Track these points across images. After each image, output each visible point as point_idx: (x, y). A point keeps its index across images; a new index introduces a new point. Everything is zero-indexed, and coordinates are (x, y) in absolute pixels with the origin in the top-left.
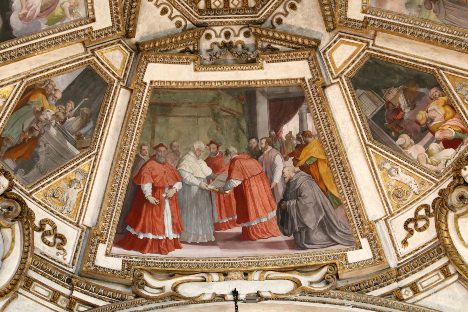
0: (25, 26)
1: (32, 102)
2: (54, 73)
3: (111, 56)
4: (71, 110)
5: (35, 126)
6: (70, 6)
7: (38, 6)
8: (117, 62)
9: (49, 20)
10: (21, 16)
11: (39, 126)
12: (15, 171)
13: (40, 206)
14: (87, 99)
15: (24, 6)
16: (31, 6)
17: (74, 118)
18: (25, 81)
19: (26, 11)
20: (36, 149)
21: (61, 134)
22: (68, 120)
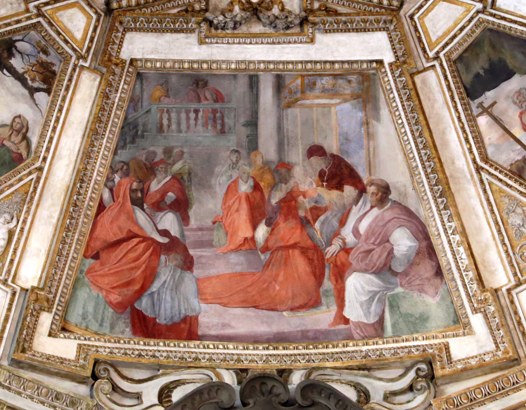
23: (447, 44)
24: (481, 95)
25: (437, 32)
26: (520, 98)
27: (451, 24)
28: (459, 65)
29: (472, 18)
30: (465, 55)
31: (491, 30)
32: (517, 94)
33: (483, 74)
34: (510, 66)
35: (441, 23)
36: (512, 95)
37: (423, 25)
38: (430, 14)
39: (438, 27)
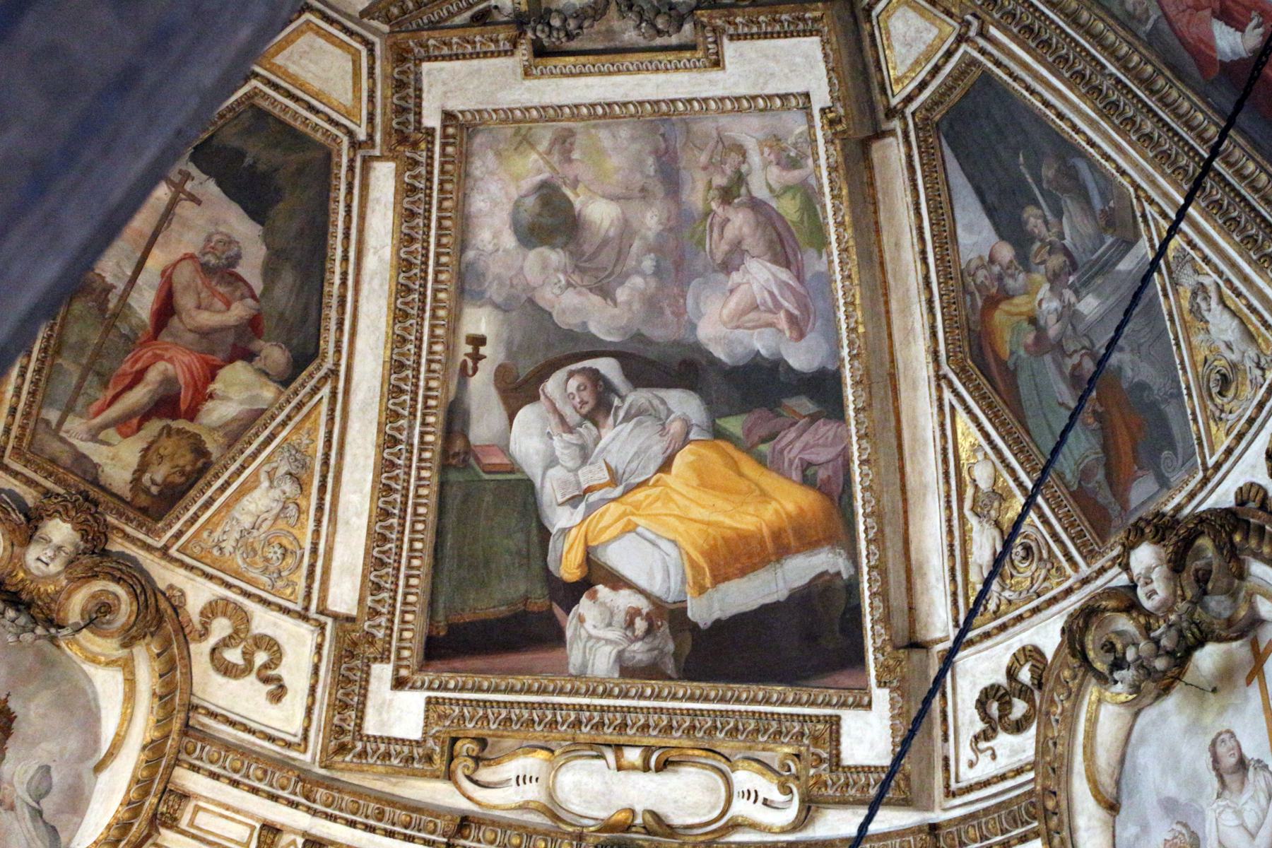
0: (818, 324)
1: (1012, 353)
2: (940, 260)
3: (903, 51)
4: (1046, 223)
5: (1069, 363)
6: (778, 164)
7: (774, 275)
8: (918, 31)
9: (811, 244)
10: (795, 335)
11: (1072, 349)
12: (1164, 483)
13: (1237, 453)
14: (1021, 158)
15: (768, 317)
16: (771, 294)
17: (1064, 220)
18: (946, 369)
19: (782, 314)
20: (1125, 386)
21: (1099, 281)
22: (1067, 242)
23: (276, 87)
24: (204, 172)
25: (294, 62)
26: (220, 246)
27: (316, 85)
28: (250, 114)
29: (337, 124)
30: (270, 120)
31: (329, 156)
32: (225, 238)
33: (245, 164)
34: (271, 213)
35: (312, 67)
36: (222, 229)
37: (299, 32)
38: (321, 41)
39: (303, 62)
